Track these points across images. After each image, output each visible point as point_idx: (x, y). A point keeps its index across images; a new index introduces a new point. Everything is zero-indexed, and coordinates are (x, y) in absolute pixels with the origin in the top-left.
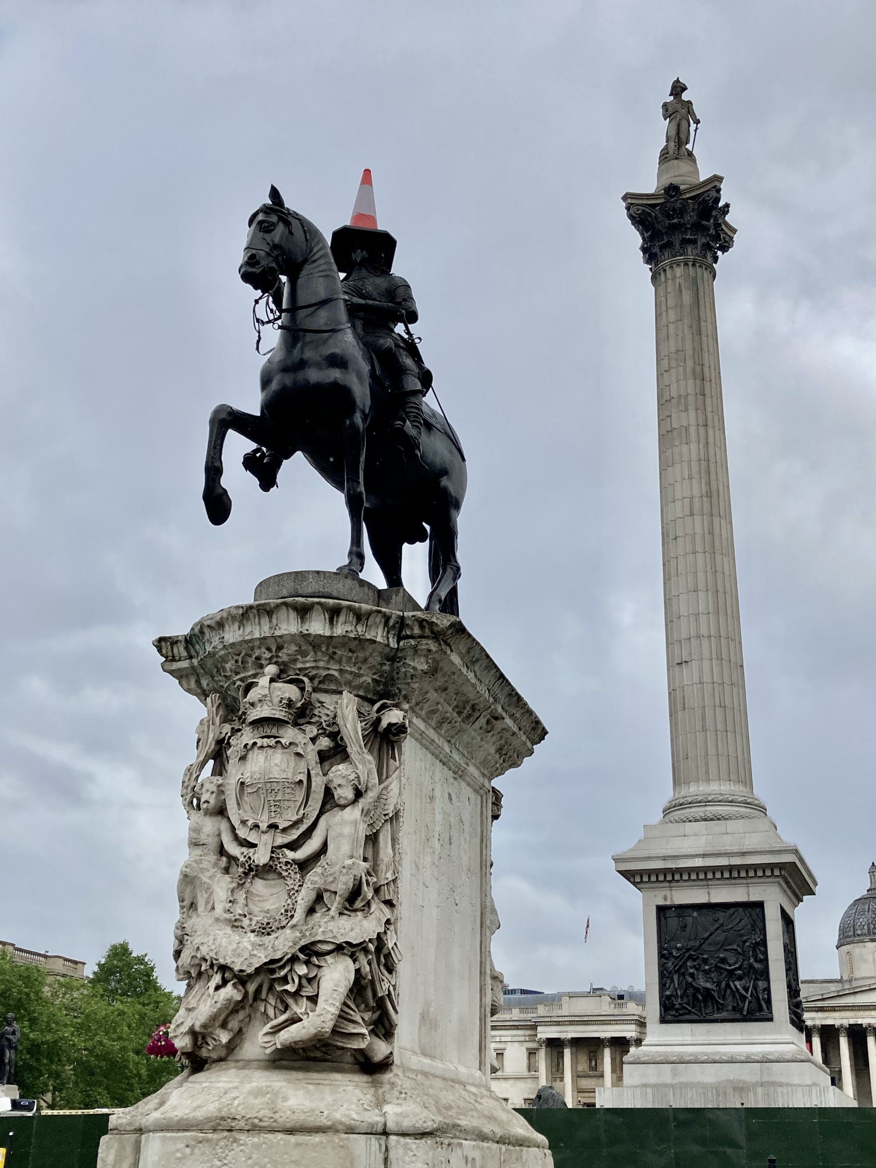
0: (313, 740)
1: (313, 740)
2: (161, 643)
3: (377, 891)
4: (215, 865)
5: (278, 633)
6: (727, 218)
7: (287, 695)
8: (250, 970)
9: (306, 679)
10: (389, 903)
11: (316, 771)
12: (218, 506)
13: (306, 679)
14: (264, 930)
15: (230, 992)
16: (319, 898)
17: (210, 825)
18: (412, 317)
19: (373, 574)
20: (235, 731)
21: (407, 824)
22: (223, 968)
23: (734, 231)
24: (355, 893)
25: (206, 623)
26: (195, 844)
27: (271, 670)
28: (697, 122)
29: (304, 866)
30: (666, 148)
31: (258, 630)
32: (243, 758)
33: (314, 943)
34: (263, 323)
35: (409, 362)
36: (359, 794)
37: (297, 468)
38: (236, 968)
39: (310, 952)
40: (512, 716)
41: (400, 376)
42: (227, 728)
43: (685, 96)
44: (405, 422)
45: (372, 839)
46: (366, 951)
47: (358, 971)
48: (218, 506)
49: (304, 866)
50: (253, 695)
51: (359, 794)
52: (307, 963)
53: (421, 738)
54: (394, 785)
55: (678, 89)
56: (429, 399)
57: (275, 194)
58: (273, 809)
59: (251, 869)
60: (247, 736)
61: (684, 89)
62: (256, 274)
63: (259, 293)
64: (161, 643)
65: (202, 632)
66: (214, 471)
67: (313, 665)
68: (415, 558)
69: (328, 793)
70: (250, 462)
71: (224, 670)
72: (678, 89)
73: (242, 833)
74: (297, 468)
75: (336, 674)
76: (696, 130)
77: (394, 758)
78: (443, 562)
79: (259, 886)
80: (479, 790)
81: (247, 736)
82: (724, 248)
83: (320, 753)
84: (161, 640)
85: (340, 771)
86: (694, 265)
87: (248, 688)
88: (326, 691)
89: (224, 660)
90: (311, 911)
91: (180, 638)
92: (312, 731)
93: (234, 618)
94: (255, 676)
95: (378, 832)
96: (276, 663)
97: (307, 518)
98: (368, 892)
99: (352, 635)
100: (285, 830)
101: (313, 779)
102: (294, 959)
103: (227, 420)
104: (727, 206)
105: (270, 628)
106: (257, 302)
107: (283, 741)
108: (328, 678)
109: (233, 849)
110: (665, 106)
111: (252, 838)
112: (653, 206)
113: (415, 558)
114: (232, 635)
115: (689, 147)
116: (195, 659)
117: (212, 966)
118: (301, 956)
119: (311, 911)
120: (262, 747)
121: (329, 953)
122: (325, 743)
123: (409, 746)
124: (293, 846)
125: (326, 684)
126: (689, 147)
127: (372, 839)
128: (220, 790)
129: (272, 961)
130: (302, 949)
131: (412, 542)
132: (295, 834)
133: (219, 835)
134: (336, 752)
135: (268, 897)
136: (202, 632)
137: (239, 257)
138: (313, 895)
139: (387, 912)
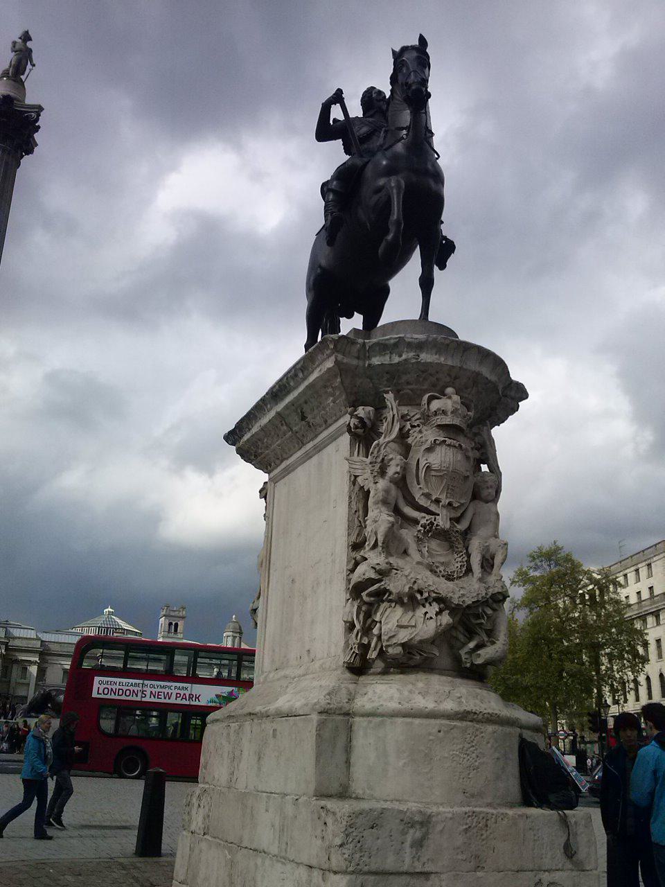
6: (36, 135)
15: (446, 619)
28: (34, 65)
30: (8, 70)
32: (430, 450)
43: (29, 44)
55: (26, 37)
58: (449, 491)
61: (30, 39)
72: (26, 37)
73: (423, 502)
76: (30, 70)
79: (434, 544)
82: (27, 154)
86: (9, 154)
110: (14, 43)
111: (433, 508)
115: (23, 77)
120: (449, 445)
126: (23, 77)
128: (405, 468)
133: (397, 499)
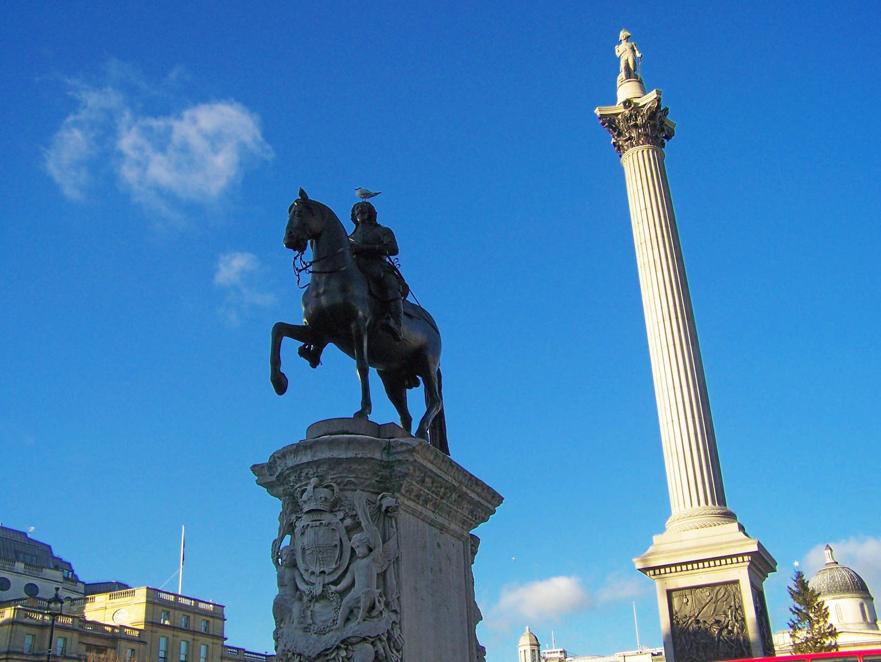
0: (342, 520)
1: (342, 520)
2: (254, 468)
3: (387, 604)
4: (294, 597)
5: (316, 459)
7: (323, 495)
8: (313, 656)
9: (334, 485)
10: (395, 611)
11: (345, 538)
12: (280, 384)
13: (334, 485)
14: (321, 632)
16: (351, 611)
17: (288, 573)
18: (395, 252)
19: (384, 412)
20: (298, 518)
21: (403, 567)
22: (300, 655)
24: (373, 607)
25: (276, 455)
26: (281, 584)
27: (314, 481)
29: (343, 593)
31: (306, 458)
32: (303, 534)
33: (348, 638)
34: (300, 271)
35: (394, 282)
36: (371, 550)
37: (331, 352)
38: (306, 654)
39: (346, 643)
40: (473, 491)
41: (388, 290)
42: (294, 517)
44: (388, 318)
45: (383, 576)
46: (380, 640)
47: (376, 652)
48: (280, 384)
49: (343, 593)
50: (305, 497)
51: (371, 550)
52: (346, 649)
53: (414, 513)
54: (392, 543)
56: (410, 298)
57: (302, 193)
59: (312, 598)
60: (305, 520)
62: (295, 243)
63: (297, 252)
64: (254, 468)
65: (275, 461)
66: (276, 361)
68: (416, 397)
69: (353, 550)
70: (303, 352)
74: (331, 352)
75: (353, 479)
77: (392, 526)
78: (433, 397)
79: (317, 607)
80: (460, 537)
81: (305, 520)
82: (668, 138)
83: (346, 528)
84: (254, 466)
85: (356, 537)
87: (304, 491)
88: (348, 490)
89: (289, 476)
90: (348, 620)
92: (341, 515)
94: (306, 485)
95: (385, 572)
97: (336, 385)
98: (380, 606)
99: (359, 456)
100: (329, 574)
101: (344, 543)
102: (338, 648)
103: (282, 331)
106: (295, 258)
107: (324, 522)
108: (350, 483)
109: (302, 587)
111: (313, 579)
113: (416, 397)
114: (291, 462)
116: (275, 475)
117: (293, 654)
118: (342, 646)
119: (348, 620)
121: (357, 643)
122: (348, 521)
123: (403, 516)
124: (336, 583)
125: (345, 486)
127: (383, 576)
129: (326, 650)
130: (343, 642)
131: (411, 388)
132: (335, 577)
133: (294, 579)
134: (356, 526)
135: (323, 612)
137: (283, 234)
138: (348, 611)
139: (394, 617)
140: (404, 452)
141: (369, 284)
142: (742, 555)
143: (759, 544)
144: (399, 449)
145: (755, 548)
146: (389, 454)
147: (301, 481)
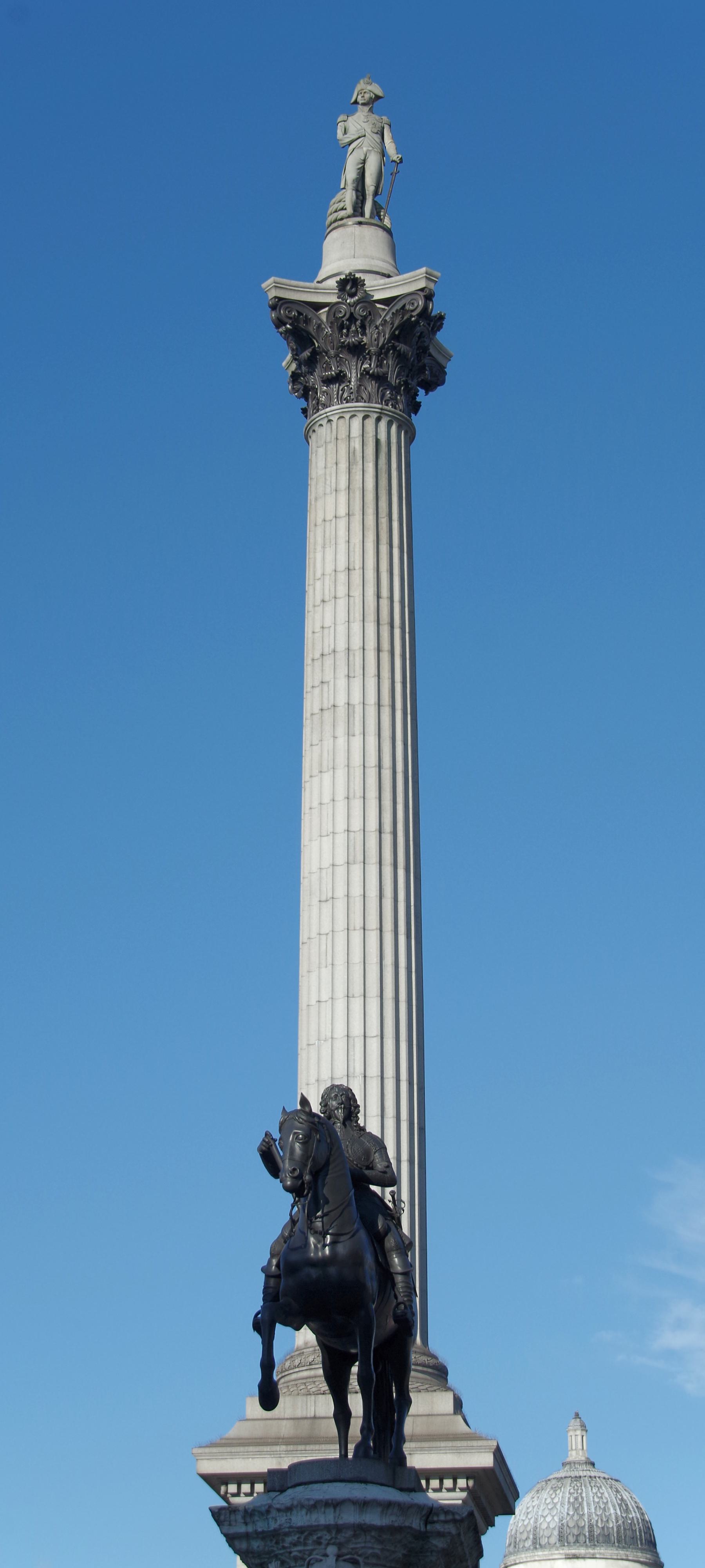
5: (340, 1522)
6: (441, 336)
23: (448, 357)
65: (268, 1512)
67: (363, 1545)
71: (283, 1541)
82: (429, 386)
89: (287, 1534)
91: (240, 1509)
93: (302, 1506)
96: (333, 1544)
99: (396, 1524)
104: (441, 318)
105: (335, 1518)
112: (317, 306)
136: (268, 1512)
140: (446, 1522)
141: (375, 1248)
142: (455, 1474)
143: (498, 1454)
144: (442, 1517)
145: (486, 1460)
146: (426, 1523)
147: (305, 1544)
